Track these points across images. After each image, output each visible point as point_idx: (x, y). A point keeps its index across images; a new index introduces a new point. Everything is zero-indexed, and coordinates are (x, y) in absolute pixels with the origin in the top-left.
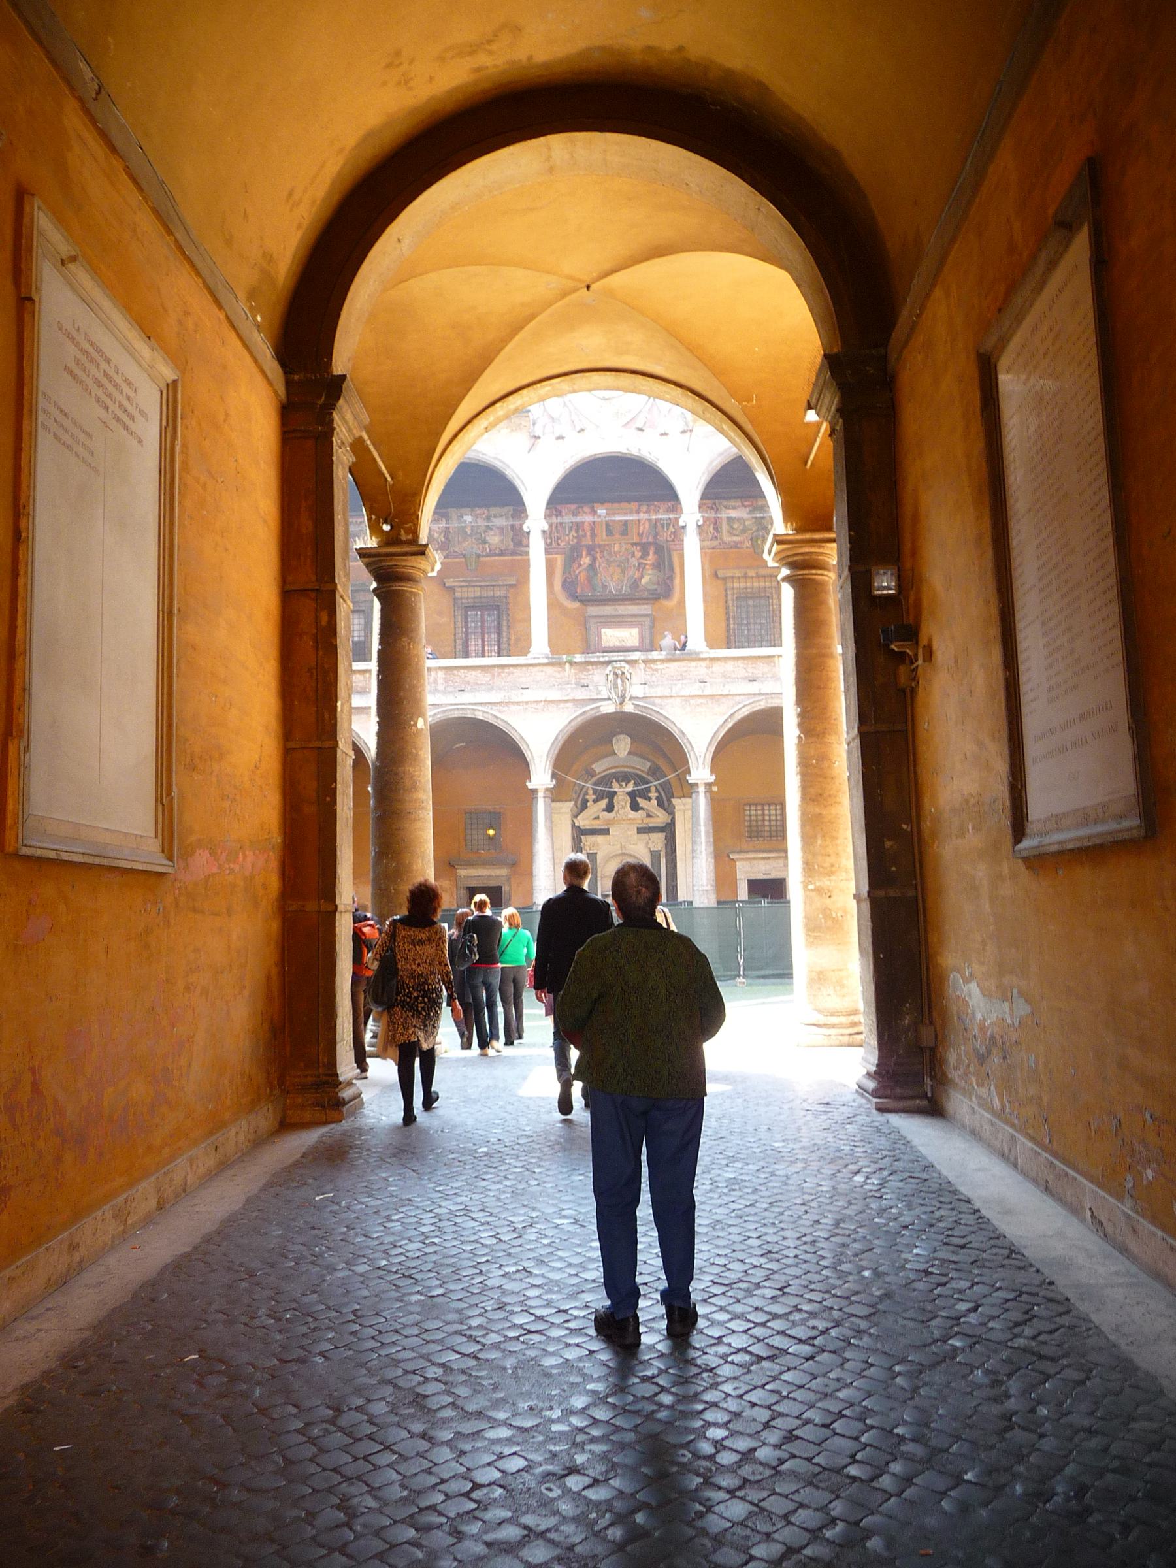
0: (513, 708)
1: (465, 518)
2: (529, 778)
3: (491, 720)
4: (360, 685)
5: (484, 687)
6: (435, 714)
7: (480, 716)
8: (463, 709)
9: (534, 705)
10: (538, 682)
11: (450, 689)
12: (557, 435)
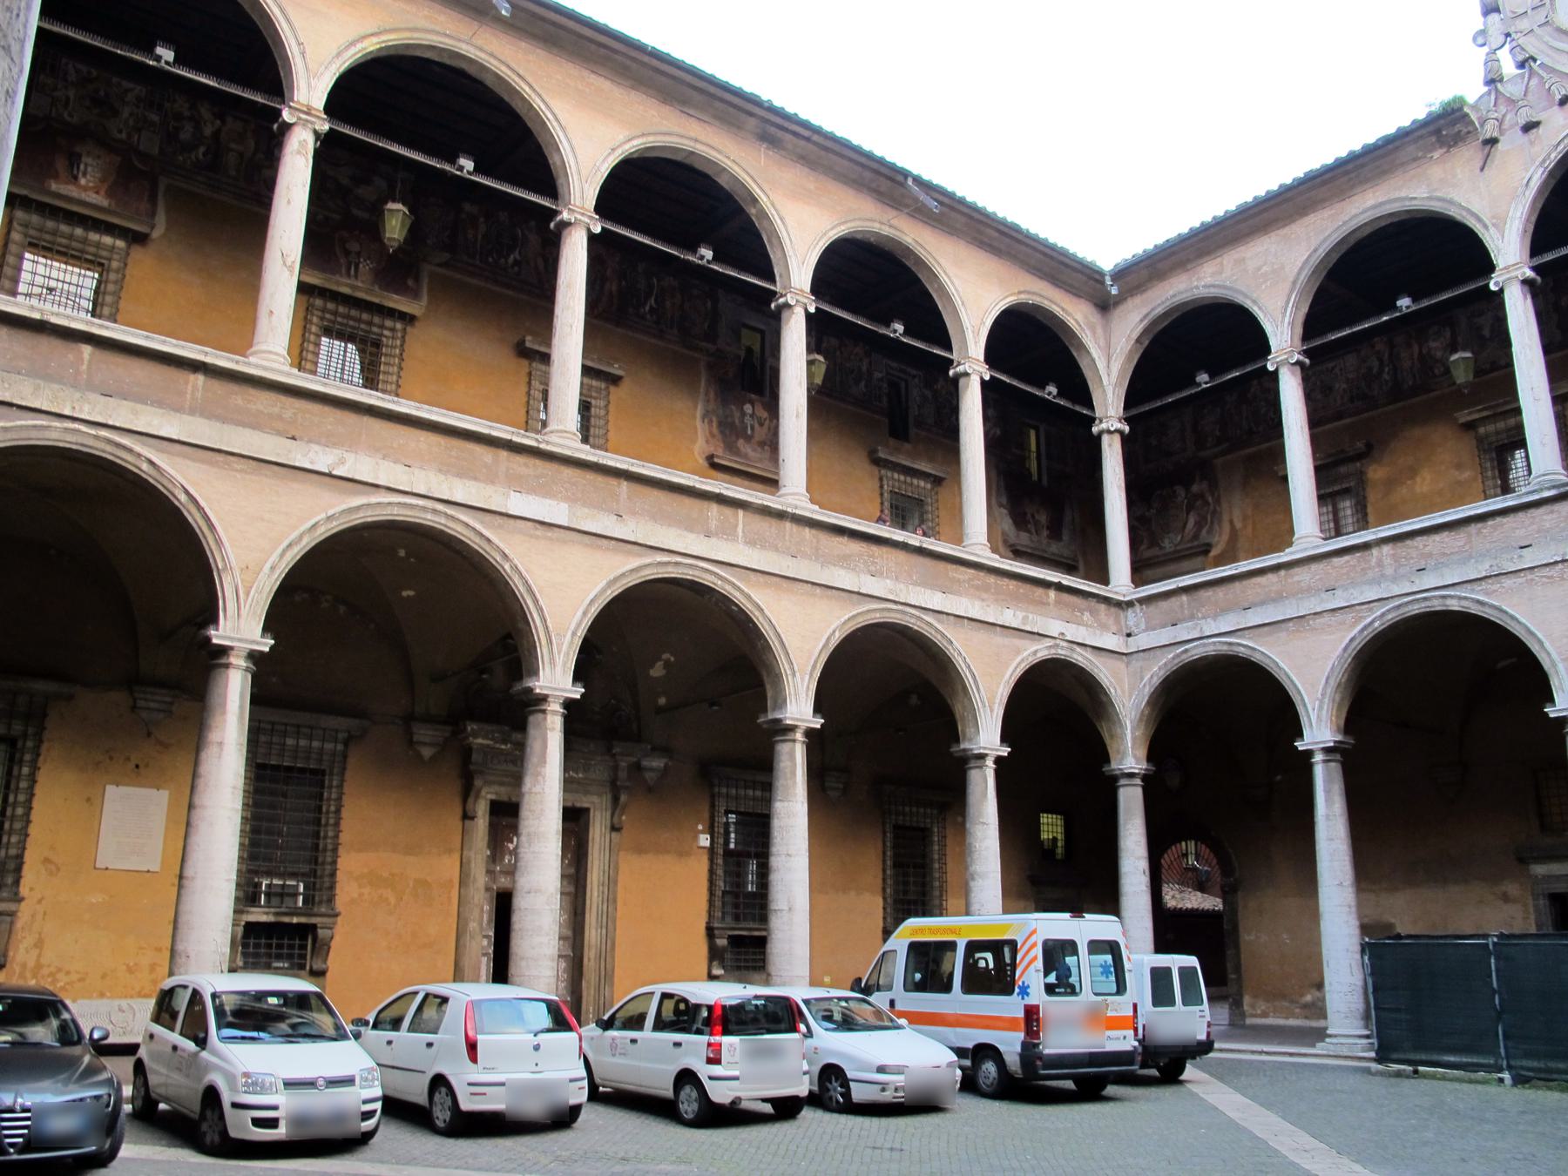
0: (1508, 582)
1: (1399, 303)
2: (1551, 700)
3: (1475, 610)
4: (1274, 588)
5: (1456, 557)
6: (1383, 615)
7: (1454, 605)
8: (1425, 599)
9: (1545, 572)
10: (1547, 531)
11: (1402, 571)
12: (1522, 122)
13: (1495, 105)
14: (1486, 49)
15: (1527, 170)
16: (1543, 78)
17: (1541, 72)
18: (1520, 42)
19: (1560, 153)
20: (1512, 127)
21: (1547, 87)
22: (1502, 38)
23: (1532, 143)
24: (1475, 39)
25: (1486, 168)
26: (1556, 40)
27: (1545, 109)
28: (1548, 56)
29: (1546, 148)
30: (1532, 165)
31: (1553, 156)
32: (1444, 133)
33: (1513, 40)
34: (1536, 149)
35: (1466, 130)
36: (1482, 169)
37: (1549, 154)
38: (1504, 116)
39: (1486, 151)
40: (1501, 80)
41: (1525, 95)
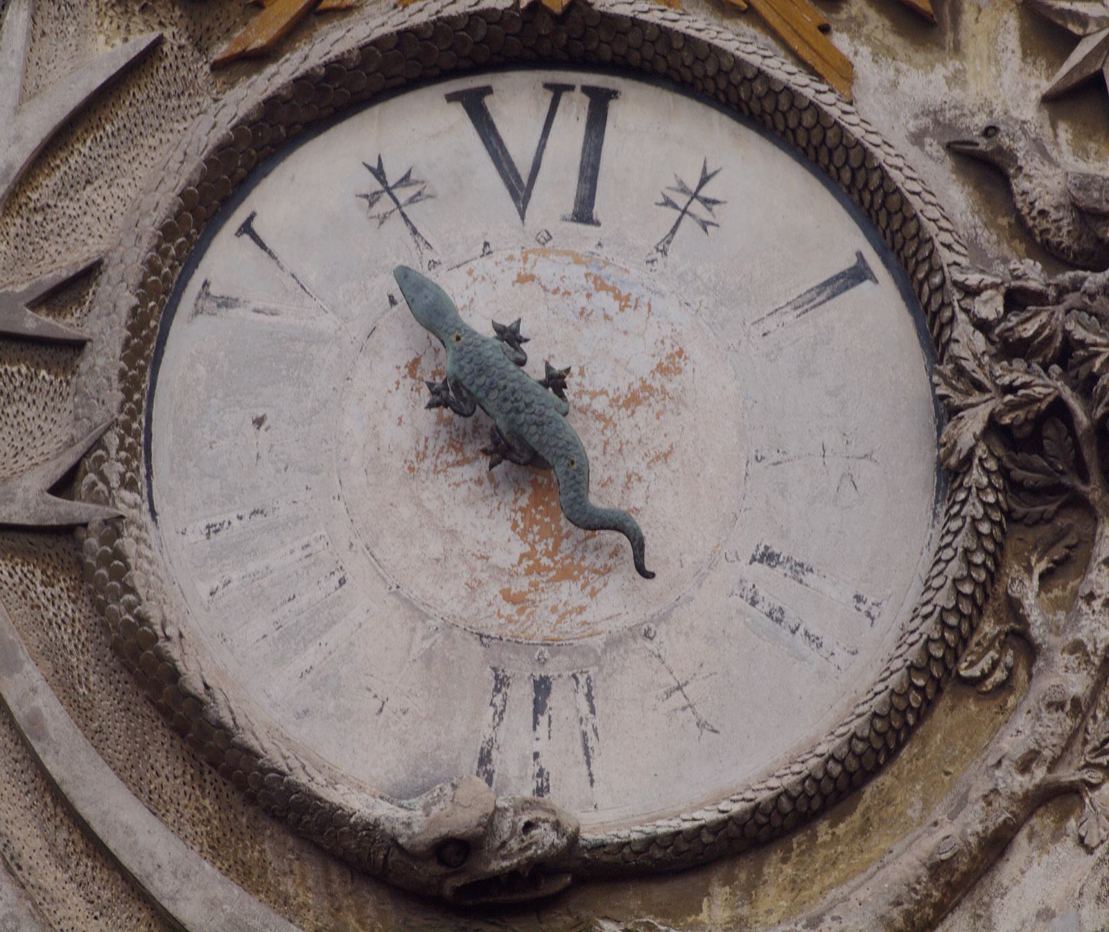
26: (97, 739)
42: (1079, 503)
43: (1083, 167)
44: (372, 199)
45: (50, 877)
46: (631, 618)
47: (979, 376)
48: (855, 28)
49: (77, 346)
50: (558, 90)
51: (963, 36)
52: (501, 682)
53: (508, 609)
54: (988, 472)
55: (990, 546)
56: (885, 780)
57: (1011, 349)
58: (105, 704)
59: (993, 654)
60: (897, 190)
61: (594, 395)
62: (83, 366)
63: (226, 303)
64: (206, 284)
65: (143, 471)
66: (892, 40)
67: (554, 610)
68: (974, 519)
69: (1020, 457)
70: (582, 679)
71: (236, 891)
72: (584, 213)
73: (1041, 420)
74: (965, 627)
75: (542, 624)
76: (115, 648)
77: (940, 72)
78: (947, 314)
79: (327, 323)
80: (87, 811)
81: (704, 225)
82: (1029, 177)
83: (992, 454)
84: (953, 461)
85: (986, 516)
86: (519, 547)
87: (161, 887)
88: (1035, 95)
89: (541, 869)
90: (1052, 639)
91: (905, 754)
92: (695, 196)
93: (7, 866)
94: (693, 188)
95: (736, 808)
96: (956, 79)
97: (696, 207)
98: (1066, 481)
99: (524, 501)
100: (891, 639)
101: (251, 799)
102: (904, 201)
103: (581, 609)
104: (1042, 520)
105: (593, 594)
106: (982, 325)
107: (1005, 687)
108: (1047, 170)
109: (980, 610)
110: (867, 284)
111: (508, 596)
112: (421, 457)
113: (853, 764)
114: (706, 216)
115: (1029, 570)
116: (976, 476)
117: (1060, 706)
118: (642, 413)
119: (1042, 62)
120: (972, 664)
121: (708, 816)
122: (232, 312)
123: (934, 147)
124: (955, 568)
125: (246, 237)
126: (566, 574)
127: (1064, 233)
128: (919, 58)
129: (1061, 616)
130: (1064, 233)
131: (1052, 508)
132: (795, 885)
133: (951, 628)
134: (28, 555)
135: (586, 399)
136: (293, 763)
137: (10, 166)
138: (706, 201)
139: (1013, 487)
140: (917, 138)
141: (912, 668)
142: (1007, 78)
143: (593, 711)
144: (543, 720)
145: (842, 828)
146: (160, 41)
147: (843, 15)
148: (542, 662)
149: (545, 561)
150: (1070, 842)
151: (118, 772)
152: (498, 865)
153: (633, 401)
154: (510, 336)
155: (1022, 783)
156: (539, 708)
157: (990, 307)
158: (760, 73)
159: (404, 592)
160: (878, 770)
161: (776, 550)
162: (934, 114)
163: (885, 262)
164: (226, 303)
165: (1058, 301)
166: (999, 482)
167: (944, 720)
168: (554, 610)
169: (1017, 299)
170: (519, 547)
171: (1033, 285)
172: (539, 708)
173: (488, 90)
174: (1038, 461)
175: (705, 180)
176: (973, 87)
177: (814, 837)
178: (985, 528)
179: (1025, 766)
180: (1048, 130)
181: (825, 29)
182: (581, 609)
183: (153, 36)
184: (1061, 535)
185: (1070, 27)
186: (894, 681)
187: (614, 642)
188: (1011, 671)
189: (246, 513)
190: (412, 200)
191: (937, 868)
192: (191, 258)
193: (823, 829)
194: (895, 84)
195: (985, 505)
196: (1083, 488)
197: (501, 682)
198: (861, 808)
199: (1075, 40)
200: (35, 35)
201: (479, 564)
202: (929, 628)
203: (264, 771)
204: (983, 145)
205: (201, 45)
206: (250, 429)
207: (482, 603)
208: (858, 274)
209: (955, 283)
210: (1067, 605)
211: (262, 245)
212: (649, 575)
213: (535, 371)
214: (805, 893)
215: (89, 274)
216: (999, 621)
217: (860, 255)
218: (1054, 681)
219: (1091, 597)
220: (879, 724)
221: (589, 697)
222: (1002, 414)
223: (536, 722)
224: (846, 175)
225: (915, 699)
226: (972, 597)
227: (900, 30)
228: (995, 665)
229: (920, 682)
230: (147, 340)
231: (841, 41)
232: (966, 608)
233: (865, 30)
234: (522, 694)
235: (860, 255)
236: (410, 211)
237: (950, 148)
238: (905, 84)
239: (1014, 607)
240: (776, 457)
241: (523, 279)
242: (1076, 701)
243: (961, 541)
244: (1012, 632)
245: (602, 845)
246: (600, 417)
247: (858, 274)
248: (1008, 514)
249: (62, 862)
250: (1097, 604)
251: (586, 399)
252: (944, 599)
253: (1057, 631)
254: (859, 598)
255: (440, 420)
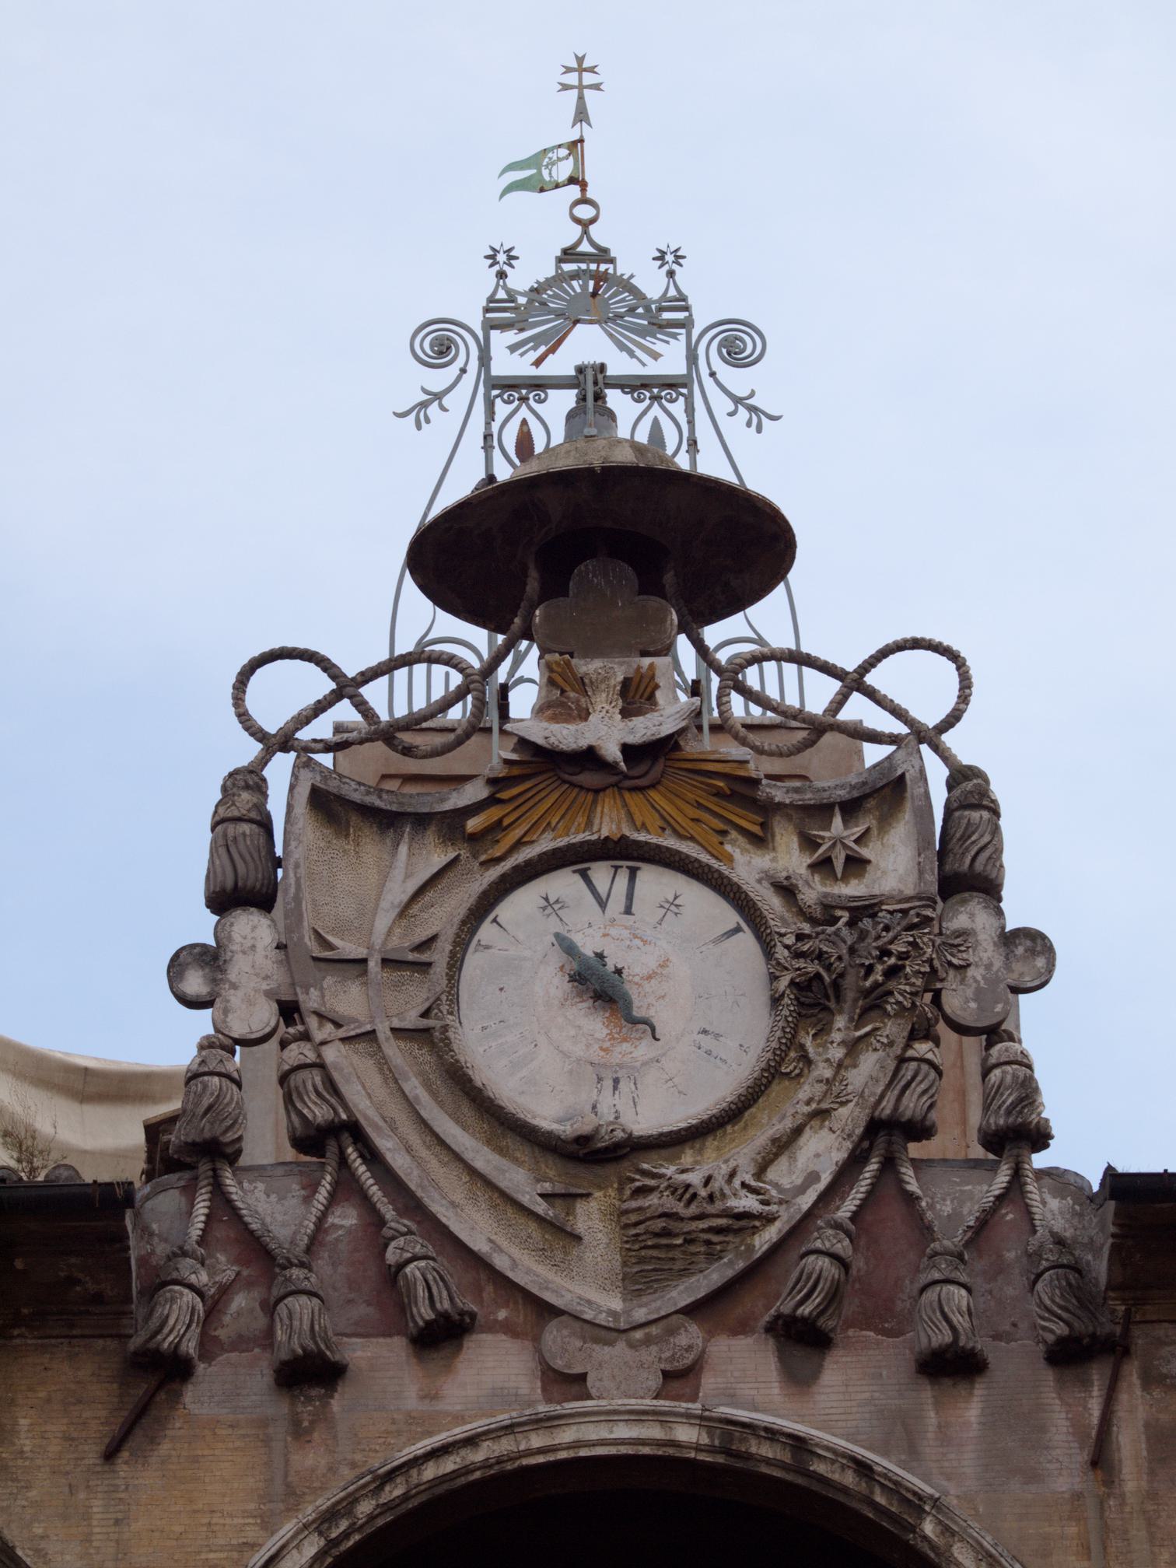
12: (291, 1341)
13: (202, 1241)
14: (202, 1023)
15: (268, 1525)
16: (380, 1222)
17: (375, 1191)
18: (330, 1054)
19: (387, 1507)
20: (240, 1343)
21: (392, 1256)
22: (262, 1016)
23: (299, 1432)
24: (177, 967)
25: (125, 1454)
26: (441, 1104)
27: (364, 1331)
28: (409, 1150)
29: (347, 1473)
30: (292, 1509)
31: (365, 1508)
32: (19, 1264)
33: (306, 1037)
34: (310, 1459)
35: (91, 1287)
36: (110, 1455)
37: (352, 1500)
38: (225, 1291)
39: (139, 1391)
40: (233, 1158)
41: (308, 1250)
42: (826, 1009)
43: (824, 890)
44: (544, 909)
45: (424, 1153)
46: (651, 1055)
47: (786, 965)
48: (733, 842)
49: (429, 965)
50: (616, 868)
51: (776, 844)
52: (600, 1080)
53: (602, 1053)
54: (791, 999)
55: (792, 1026)
56: (753, 1110)
57: (799, 955)
58: (443, 1091)
59: (794, 1064)
60: (752, 900)
61: (634, 976)
62: (432, 972)
63: (487, 947)
64: (479, 941)
65: (456, 1008)
66: (748, 846)
67: (620, 1053)
68: (786, 1016)
69: (804, 993)
70: (632, 1078)
71: (497, 1157)
72: (628, 911)
73: (811, 980)
74: (783, 1055)
75: (616, 1058)
76: (447, 1072)
77: (768, 857)
78: (773, 943)
79: (527, 953)
80: (438, 1130)
81: (676, 914)
82: (803, 894)
83: (792, 993)
84: (777, 995)
85: (791, 1015)
86: (606, 1031)
87: (468, 1156)
88: (805, 865)
89: (617, 1146)
90: (818, 1058)
91: (761, 1100)
92: (672, 904)
93: (407, 1150)
94: (671, 900)
95: (694, 1122)
96: (774, 860)
97: (673, 908)
98: (821, 1001)
99: (607, 1015)
100: (754, 1061)
101: (502, 1124)
102: (755, 903)
103: (631, 1053)
104: (813, 1015)
105: (635, 1047)
106: (787, 947)
107: (799, 1075)
108: (810, 891)
109: (789, 1048)
110: (741, 934)
111: (601, 1049)
112: (566, 1000)
113: (740, 1105)
114: (676, 911)
115: (808, 1033)
116: (786, 1000)
117: (821, 1081)
118: (653, 981)
119: (808, 853)
120: (786, 1068)
121: (683, 1125)
122: (490, 951)
123: (766, 884)
124: (779, 1034)
125: (495, 924)
126: (625, 1040)
127: (818, 913)
128: (759, 852)
129: (821, 1049)
130: (818, 913)
131: (817, 1011)
132: (718, 1149)
133: (778, 1055)
134: (412, 1039)
135: (631, 978)
136: (519, 1111)
137: (401, 902)
138: (677, 906)
139: (801, 1004)
140: (759, 881)
141: (763, 1070)
142: (794, 859)
143: (636, 1088)
144: (617, 1092)
145: (736, 1128)
146: (458, 856)
147: (729, 838)
148: (616, 1072)
149: (616, 1036)
150: (826, 1130)
151: (450, 1116)
152: (600, 1145)
153: (649, 978)
154: (600, 956)
155: (807, 1109)
156: (615, 1088)
157: (790, 940)
158: (696, 860)
159: (560, 1049)
160: (750, 1106)
161: (707, 1029)
162: (766, 872)
163: (748, 925)
164: (487, 947)
165: (816, 937)
166: (795, 1003)
167: (775, 1087)
168: (620, 1053)
169: (800, 937)
170: (606, 1031)
171: (806, 932)
172: (615, 1088)
173: (589, 869)
174: (809, 994)
175: (676, 898)
176: (781, 862)
177: (726, 1131)
178: (790, 1019)
179: (808, 1103)
180: (810, 877)
181: (722, 843)
182: (631, 1053)
183: (456, 854)
184: (820, 1021)
185: (818, 840)
186: (756, 1075)
187: (644, 1064)
188: (802, 1070)
189: (497, 1022)
190: (560, 909)
191: (774, 1141)
192: (473, 931)
193: (729, 1128)
194: (750, 862)
195: (790, 1011)
196: (827, 1003)
197: (600, 1080)
198: (744, 1120)
199: (820, 845)
200: (410, 854)
201: (590, 1038)
202: (769, 1055)
203: (507, 1114)
204: (785, 883)
205: (475, 856)
206: (498, 992)
207: (591, 1052)
208: (738, 930)
209: (776, 932)
210: (824, 1045)
211: (501, 927)
212: (658, 1040)
213: (610, 968)
214: (722, 1152)
215: (433, 939)
216: (796, 1052)
217: (738, 923)
218: (818, 1073)
219: (832, 1042)
220: (750, 1090)
221: (635, 1084)
222: (795, 978)
223: (614, 1093)
224: (732, 895)
225: (764, 1081)
226: (786, 1044)
227: (751, 842)
228: (795, 1068)
229: (766, 1075)
230: (456, 961)
231: (728, 848)
232: (783, 1048)
233: (738, 843)
234: (608, 1083)
235: (738, 923)
236: (559, 912)
237: (772, 884)
238: (753, 862)
239: (802, 1047)
240: (706, 996)
241: (605, 935)
242: (827, 1080)
243: (781, 1024)
244: (802, 1056)
245: (642, 1137)
246: (637, 984)
247: (738, 930)
248: (799, 1014)
249: (429, 1148)
250: (835, 1045)
251: (631, 978)
252: (775, 1045)
253: (820, 1055)
254: (741, 1046)
255: (573, 987)
